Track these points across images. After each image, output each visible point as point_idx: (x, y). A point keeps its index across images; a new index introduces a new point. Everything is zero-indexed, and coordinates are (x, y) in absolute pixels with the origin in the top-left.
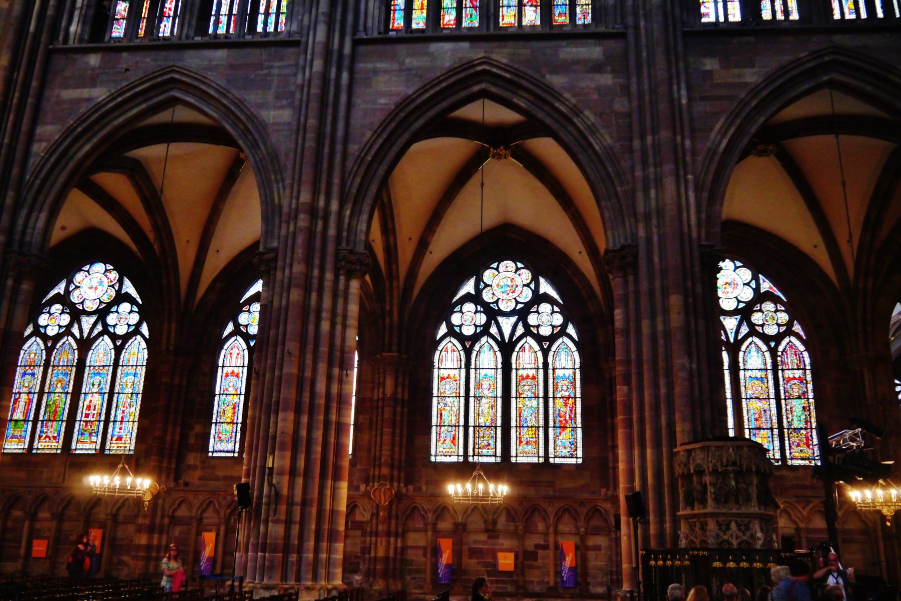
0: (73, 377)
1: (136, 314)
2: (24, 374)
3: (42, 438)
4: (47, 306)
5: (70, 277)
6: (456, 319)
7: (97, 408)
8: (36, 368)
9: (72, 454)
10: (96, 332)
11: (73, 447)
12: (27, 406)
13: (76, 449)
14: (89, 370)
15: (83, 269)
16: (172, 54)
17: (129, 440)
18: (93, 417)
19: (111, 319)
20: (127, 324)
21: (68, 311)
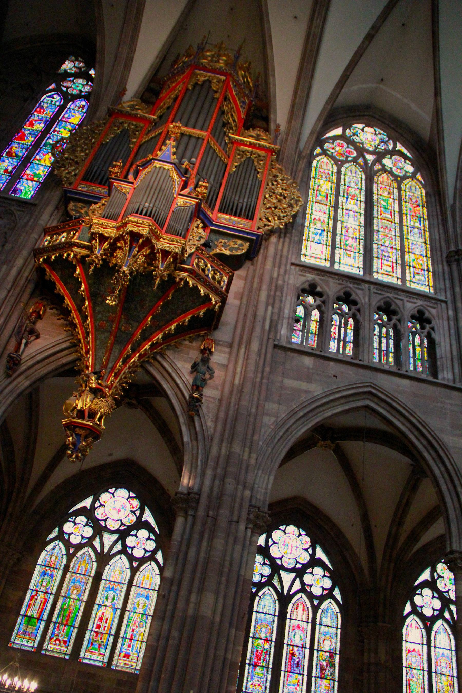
0: (89, 586)
1: (153, 542)
2: (45, 574)
3: (53, 640)
4: (73, 516)
5: (97, 495)
6: (418, 600)
7: (108, 621)
8: (55, 570)
9: (80, 662)
10: (115, 550)
11: (82, 655)
12: (42, 605)
13: (84, 658)
14: (105, 584)
15: (109, 490)
16: (368, 373)
17: (136, 659)
18: (104, 630)
19: (130, 541)
20: (144, 549)
21: (92, 525)
